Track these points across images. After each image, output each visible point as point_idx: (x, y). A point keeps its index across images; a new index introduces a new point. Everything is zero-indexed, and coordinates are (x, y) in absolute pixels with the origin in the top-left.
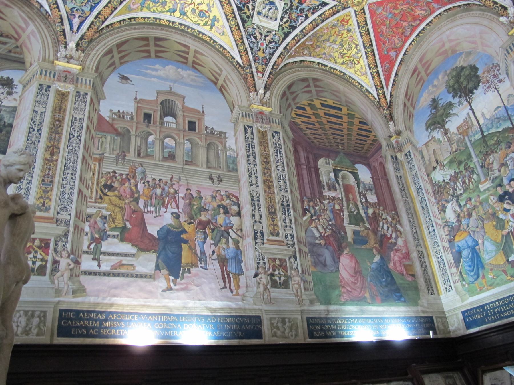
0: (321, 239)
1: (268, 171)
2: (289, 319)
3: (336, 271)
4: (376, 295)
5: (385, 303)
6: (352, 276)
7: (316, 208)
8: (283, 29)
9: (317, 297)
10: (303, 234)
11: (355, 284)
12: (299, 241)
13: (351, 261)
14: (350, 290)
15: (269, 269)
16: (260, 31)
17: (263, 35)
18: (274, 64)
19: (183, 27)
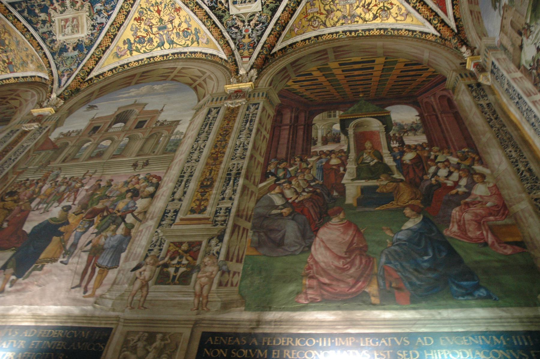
0: (285, 207)
1: (224, 142)
2: (165, 334)
3: (303, 252)
4: (398, 289)
5: (424, 304)
6: (340, 258)
7: (290, 169)
8: (268, 6)
9: (243, 297)
10: (252, 205)
11: (343, 270)
12: (238, 215)
13: (344, 233)
14: (327, 281)
15: (163, 258)
16: (241, 19)
17: (246, 21)
18: (265, 43)
19: (176, 55)
